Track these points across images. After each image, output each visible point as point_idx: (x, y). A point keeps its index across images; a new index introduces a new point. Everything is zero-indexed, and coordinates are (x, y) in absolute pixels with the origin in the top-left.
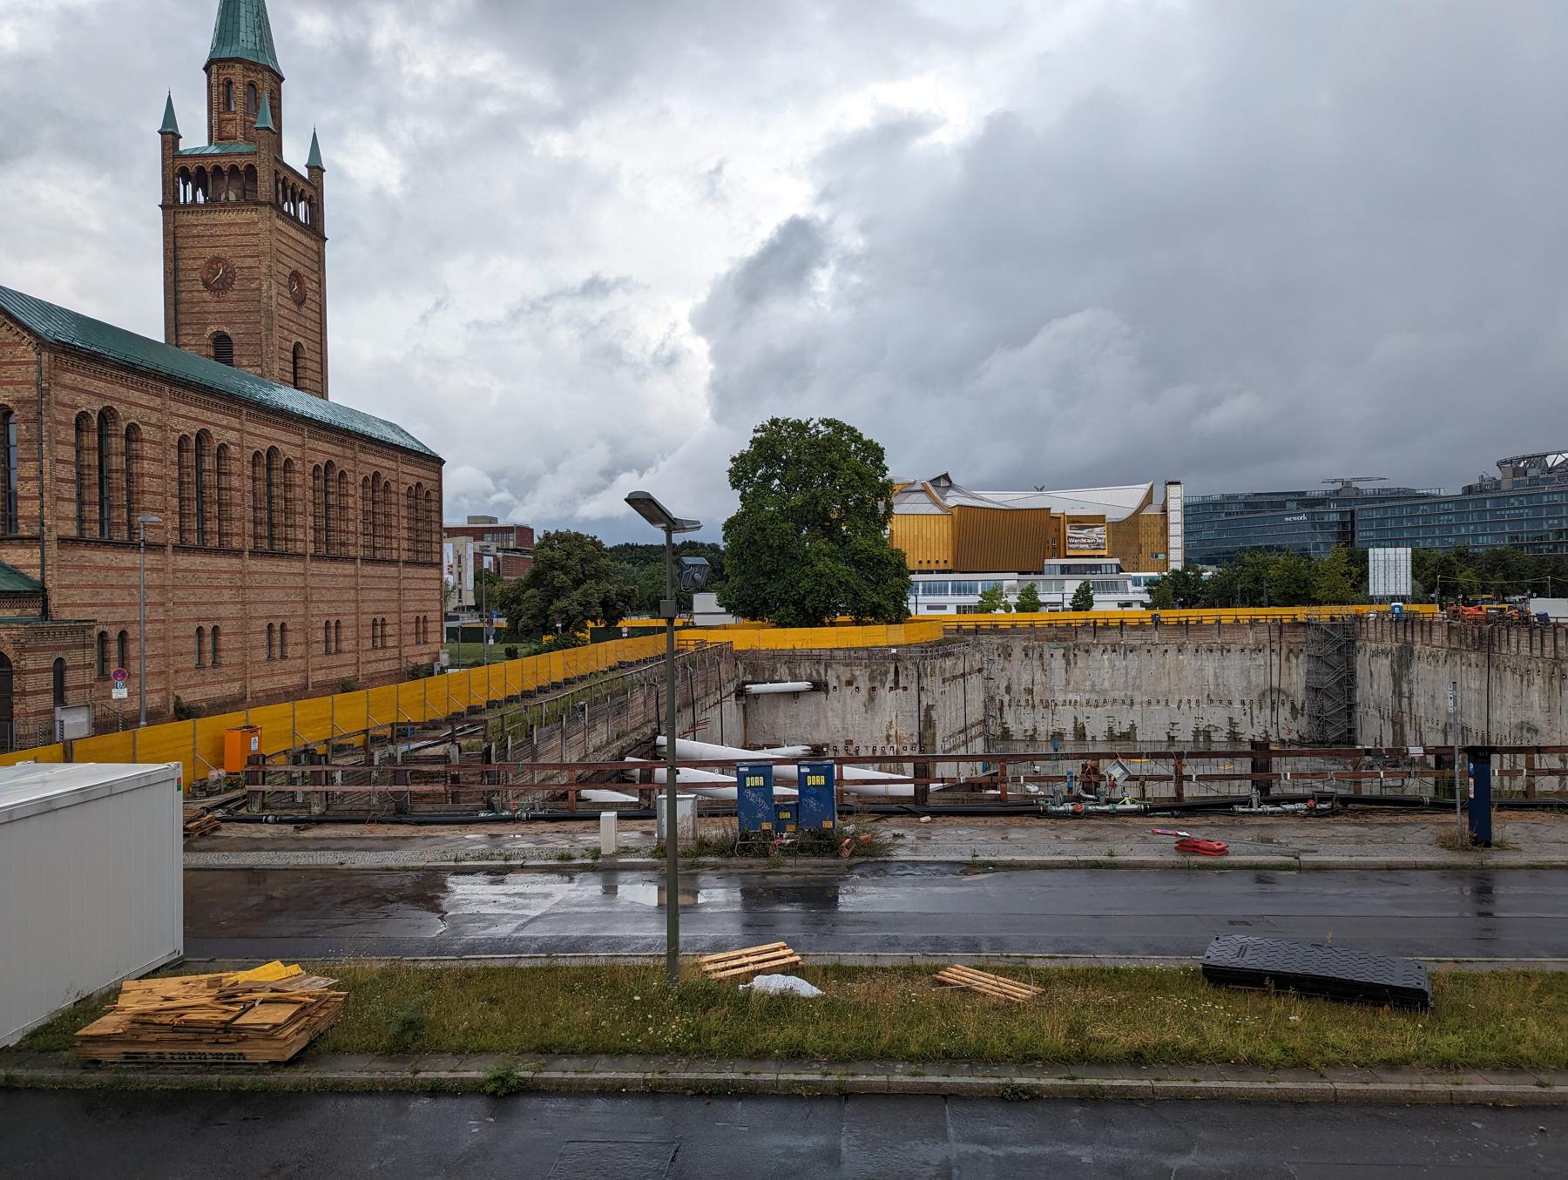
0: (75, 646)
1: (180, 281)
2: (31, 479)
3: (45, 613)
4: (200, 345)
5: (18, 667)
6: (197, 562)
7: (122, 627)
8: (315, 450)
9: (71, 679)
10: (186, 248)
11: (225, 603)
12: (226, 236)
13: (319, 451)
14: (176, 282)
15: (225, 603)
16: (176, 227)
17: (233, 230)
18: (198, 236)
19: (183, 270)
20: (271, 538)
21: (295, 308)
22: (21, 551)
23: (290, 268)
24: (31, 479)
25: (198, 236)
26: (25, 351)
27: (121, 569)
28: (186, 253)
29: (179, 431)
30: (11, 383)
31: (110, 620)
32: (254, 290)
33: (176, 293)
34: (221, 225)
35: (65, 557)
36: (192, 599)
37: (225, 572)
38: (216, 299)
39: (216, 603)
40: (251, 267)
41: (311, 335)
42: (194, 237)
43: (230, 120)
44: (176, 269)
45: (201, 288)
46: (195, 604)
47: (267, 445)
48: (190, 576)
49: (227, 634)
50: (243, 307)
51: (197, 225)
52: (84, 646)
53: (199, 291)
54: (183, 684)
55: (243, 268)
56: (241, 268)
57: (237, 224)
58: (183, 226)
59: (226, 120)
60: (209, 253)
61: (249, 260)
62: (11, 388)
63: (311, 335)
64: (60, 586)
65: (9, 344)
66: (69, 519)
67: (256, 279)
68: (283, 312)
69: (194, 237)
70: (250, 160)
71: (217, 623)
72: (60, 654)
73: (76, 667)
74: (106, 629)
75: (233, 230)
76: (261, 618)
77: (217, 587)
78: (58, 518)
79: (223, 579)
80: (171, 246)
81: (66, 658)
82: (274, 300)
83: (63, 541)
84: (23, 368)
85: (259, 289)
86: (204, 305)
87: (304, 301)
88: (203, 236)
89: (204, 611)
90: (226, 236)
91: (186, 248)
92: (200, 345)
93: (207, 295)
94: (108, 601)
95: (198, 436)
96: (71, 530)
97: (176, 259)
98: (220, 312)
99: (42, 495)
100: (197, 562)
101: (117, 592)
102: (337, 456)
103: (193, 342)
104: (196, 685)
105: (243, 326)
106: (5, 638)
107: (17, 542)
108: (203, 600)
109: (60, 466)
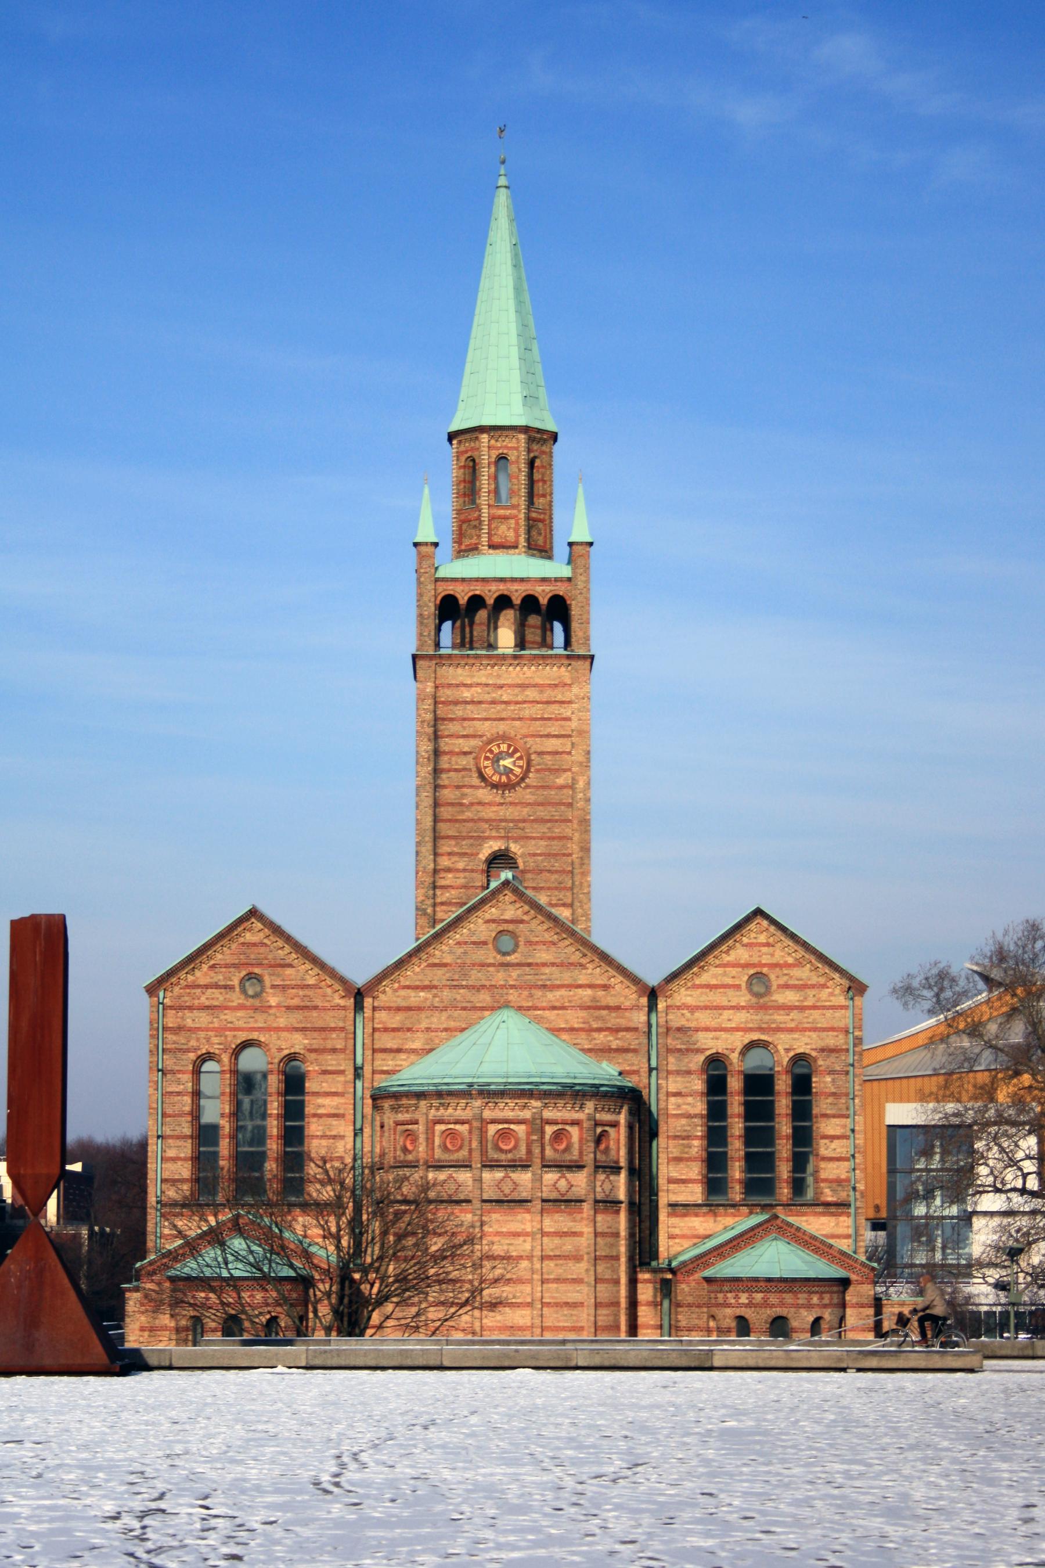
1: (442, 771)
2: (838, 1137)
4: (472, 871)
10: (452, 720)
12: (517, 703)
14: (436, 772)
16: (436, 687)
17: (531, 694)
18: (472, 702)
19: (445, 753)
22: (824, 1219)
24: (838, 1137)
25: (472, 702)
26: (832, 994)
28: (453, 728)
30: (815, 1029)
32: (562, 787)
33: (436, 787)
38: (498, 799)
40: (557, 753)
42: (466, 703)
43: (506, 518)
44: (437, 753)
45: (476, 781)
50: (542, 812)
51: (470, 686)
56: (540, 754)
57: (535, 686)
58: (450, 686)
59: (500, 517)
60: (487, 728)
62: (814, 1035)
65: (813, 986)
67: (565, 770)
69: (466, 703)
70: (561, 590)
75: (531, 694)
80: (429, 716)
84: (829, 1013)
85: (572, 787)
86: (480, 808)
88: (480, 702)
90: (517, 703)
91: (452, 720)
92: (472, 871)
93: (484, 794)
97: (436, 737)
99: (853, 1156)
103: (461, 865)
105: (543, 843)
107: (820, 1209)
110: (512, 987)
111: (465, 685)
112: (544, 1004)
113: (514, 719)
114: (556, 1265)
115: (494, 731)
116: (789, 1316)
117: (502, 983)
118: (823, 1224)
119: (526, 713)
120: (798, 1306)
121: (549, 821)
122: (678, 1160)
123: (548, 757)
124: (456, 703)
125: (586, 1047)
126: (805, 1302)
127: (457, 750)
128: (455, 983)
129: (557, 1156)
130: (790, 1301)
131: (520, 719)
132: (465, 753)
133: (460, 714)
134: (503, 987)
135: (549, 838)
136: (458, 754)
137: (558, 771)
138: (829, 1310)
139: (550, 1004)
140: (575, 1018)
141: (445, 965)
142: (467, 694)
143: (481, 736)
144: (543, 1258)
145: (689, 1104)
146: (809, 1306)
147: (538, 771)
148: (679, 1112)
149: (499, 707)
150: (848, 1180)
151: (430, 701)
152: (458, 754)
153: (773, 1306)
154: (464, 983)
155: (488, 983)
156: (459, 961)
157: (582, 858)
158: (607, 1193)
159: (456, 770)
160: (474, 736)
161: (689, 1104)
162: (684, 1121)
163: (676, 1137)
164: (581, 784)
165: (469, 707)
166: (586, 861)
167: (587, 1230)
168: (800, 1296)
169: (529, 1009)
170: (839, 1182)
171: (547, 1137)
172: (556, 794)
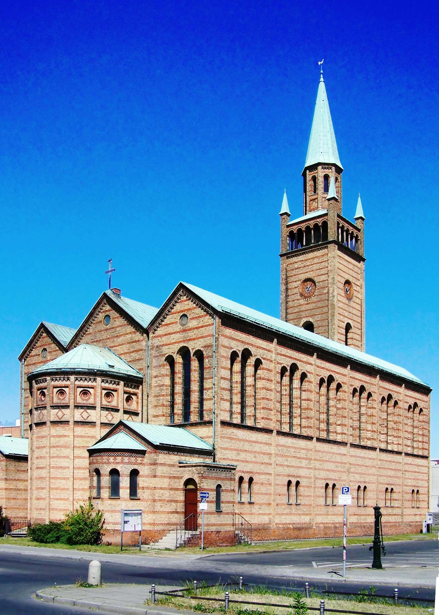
0: (227, 479)
3: (214, 461)
5: (200, 487)
6: (289, 442)
7: (251, 475)
8: (354, 378)
9: (224, 496)
10: (292, 276)
11: (303, 468)
13: (356, 379)
15: (303, 468)
20: (328, 431)
21: (346, 301)
23: (344, 278)
27: (250, 441)
29: (281, 364)
31: (245, 470)
34: (309, 259)
35: (224, 432)
36: (286, 463)
37: (303, 449)
39: (298, 467)
40: (324, 281)
41: (356, 318)
42: (296, 269)
46: (288, 466)
47: (328, 374)
48: (285, 449)
49: (303, 486)
50: (320, 304)
52: (231, 479)
53: (298, 300)
54: (280, 512)
55: (320, 282)
60: (303, 277)
61: (323, 276)
63: (356, 318)
64: (222, 448)
66: (225, 410)
68: (341, 305)
69: (296, 269)
71: (299, 479)
72: (219, 482)
73: (227, 491)
74: (243, 475)
76: (322, 479)
77: (299, 458)
78: (221, 410)
79: (302, 453)
81: (222, 485)
82: (335, 298)
83: (224, 423)
87: (352, 298)
88: (300, 268)
89: (292, 471)
91: (292, 276)
94: (243, 459)
95: (291, 367)
96: (226, 417)
98: (308, 310)
100: (289, 442)
101: (248, 454)
102: (366, 382)
104: (287, 514)
106: (195, 471)
108: (292, 464)
109: (222, 381)
110: (108, 338)
111: (296, 262)
112: (117, 344)
113: (310, 271)
114: (57, 450)
115: (304, 278)
116: (99, 468)
117: (106, 337)
118: (204, 432)
119: (315, 268)
120: (103, 463)
121: (322, 307)
122: (156, 406)
123: (321, 283)
124: (292, 270)
125: (129, 360)
126: (106, 461)
127: (293, 287)
128: (93, 341)
129: (59, 401)
130: (100, 461)
131: (312, 271)
132: (296, 288)
133: (294, 273)
134: (106, 339)
135: (322, 314)
136: (294, 288)
137: (323, 288)
138: (121, 465)
139: (119, 344)
140: (125, 348)
141: (90, 334)
142: (296, 266)
143: (300, 280)
144: (50, 447)
145: (160, 380)
146: (109, 463)
147: (318, 289)
148: (157, 385)
149: (306, 268)
150: (212, 409)
151: (285, 271)
152: (294, 288)
153: (94, 463)
154: (95, 340)
155: (101, 339)
156: (94, 331)
157: (331, 319)
158: (85, 418)
159: (293, 294)
160: (298, 281)
161: (160, 380)
162: (158, 388)
163: (155, 396)
164: (331, 291)
165: (297, 270)
166: (333, 320)
167: (71, 434)
168: (104, 458)
169: (113, 347)
170: (210, 410)
171: (55, 393)
172: (324, 297)
